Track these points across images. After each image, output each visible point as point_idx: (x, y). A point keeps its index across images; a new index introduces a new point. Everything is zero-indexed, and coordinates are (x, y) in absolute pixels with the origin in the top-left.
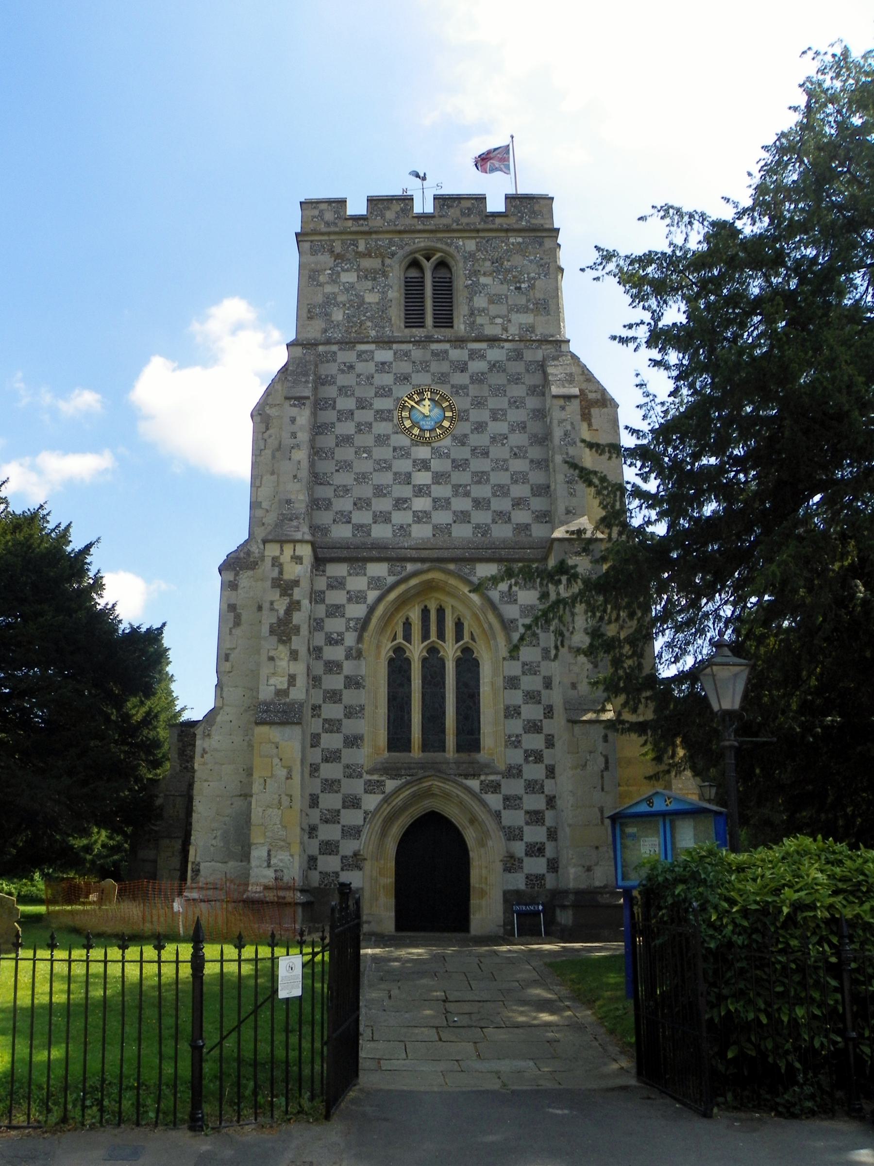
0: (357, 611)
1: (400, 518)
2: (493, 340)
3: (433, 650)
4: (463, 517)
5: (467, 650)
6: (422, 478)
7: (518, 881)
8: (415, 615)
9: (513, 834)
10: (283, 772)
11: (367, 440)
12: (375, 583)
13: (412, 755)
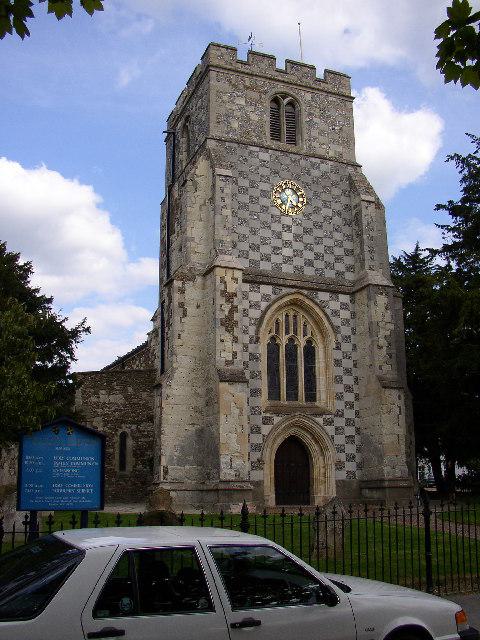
0: (255, 314)
1: (275, 259)
2: (323, 158)
3: (291, 340)
4: (309, 263)
5: (309, 342)
6: (287, 236)
7: (342, 475)
8: (282, 319)
9: (340, 449)
10: (237, 411)
11: (256, 208)
12: (265, 297)
13: (317, 404)
